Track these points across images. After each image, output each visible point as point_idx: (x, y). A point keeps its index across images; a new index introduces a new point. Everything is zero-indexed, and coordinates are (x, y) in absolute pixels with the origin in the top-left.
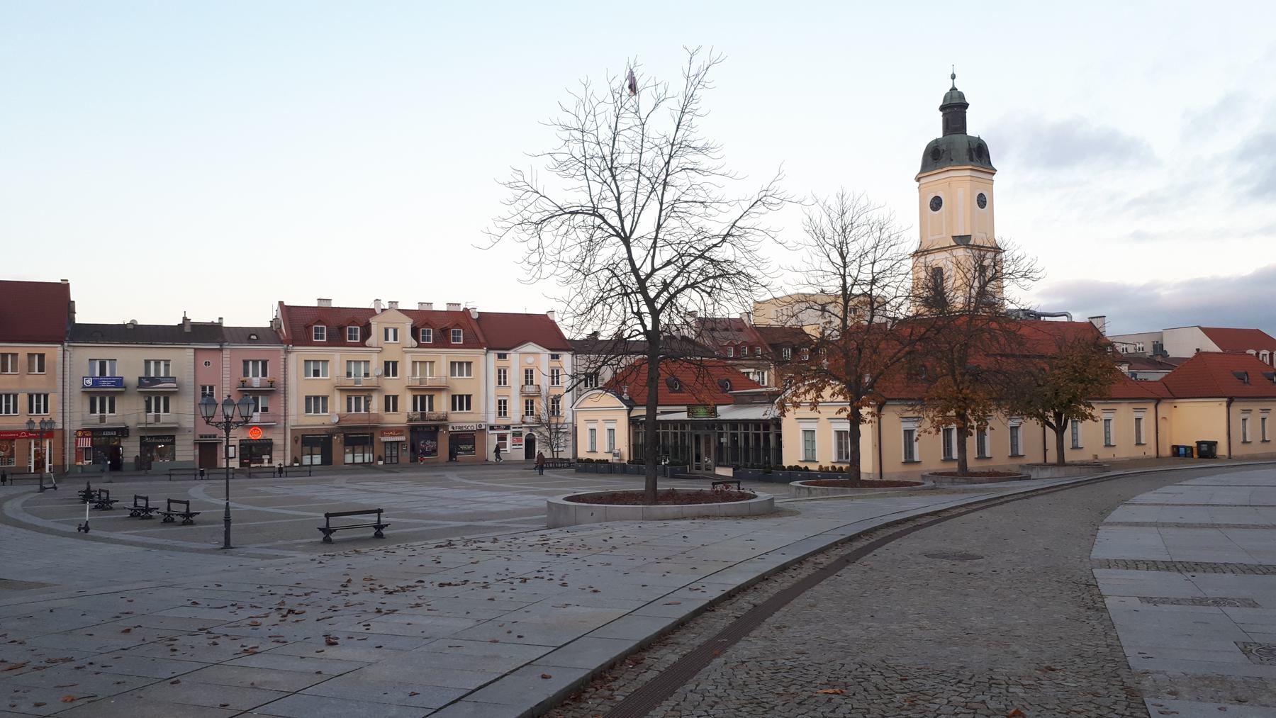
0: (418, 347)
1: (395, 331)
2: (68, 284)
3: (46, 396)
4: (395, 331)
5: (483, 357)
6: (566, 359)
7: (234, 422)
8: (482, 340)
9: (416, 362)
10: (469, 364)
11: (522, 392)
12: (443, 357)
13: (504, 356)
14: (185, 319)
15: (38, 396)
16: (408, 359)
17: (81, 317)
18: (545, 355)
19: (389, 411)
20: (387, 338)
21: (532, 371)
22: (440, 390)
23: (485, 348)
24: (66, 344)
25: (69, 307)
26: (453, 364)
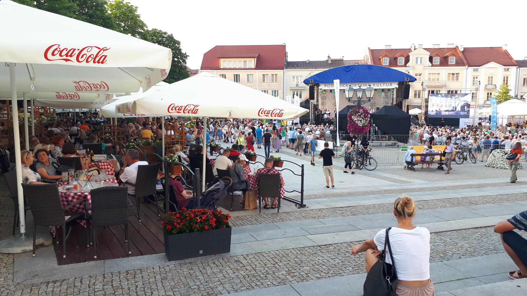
1: (421, 58)
2: (285, 45)
3: (278, 91)
4: (421, 58)
6: (513, 69)
7: (363, 101)
8: (465, 62)
9: (430, 74)
11: (486, 89)
13: (477, 70)
14: (329, 57)
15: (275, 91)
16: (427, 72)
17: (290, 59)
20: (417, 63)
21: (492, 77)
24: (284, 70)
25: (285, 54)
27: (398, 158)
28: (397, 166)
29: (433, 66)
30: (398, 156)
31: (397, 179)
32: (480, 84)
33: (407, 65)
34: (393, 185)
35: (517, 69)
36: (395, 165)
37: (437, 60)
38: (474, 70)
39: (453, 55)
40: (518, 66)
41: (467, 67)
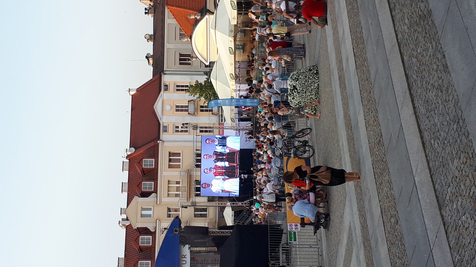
0: (156, 192)
5: (165, 144)
6: (166, 79)
8: (152, 144)
9: (168, 194)
10: (170, 154)
11: (194, 114)
12: (165, 173)
13: (165, 127)
16: (166, 200)
18: (164, 95)
19: (206, 214)
20: (150, 216)
21: (177, 106)
22: (190, 177)
23: (158, 142)
26: (170, 166)
27: (308, 246)
28: (322, 248)
29: (155, 191)
30: (306, 246)
31: (346, 250)
32: (187, 124)
33: (152, 230)
34: (358, 257)
35: (165, 74)
36: (322, 251)
37: (147, 185)
38: (165, 131)
39: (140, 162)
40: (162, 73)
41: (161, 142)
